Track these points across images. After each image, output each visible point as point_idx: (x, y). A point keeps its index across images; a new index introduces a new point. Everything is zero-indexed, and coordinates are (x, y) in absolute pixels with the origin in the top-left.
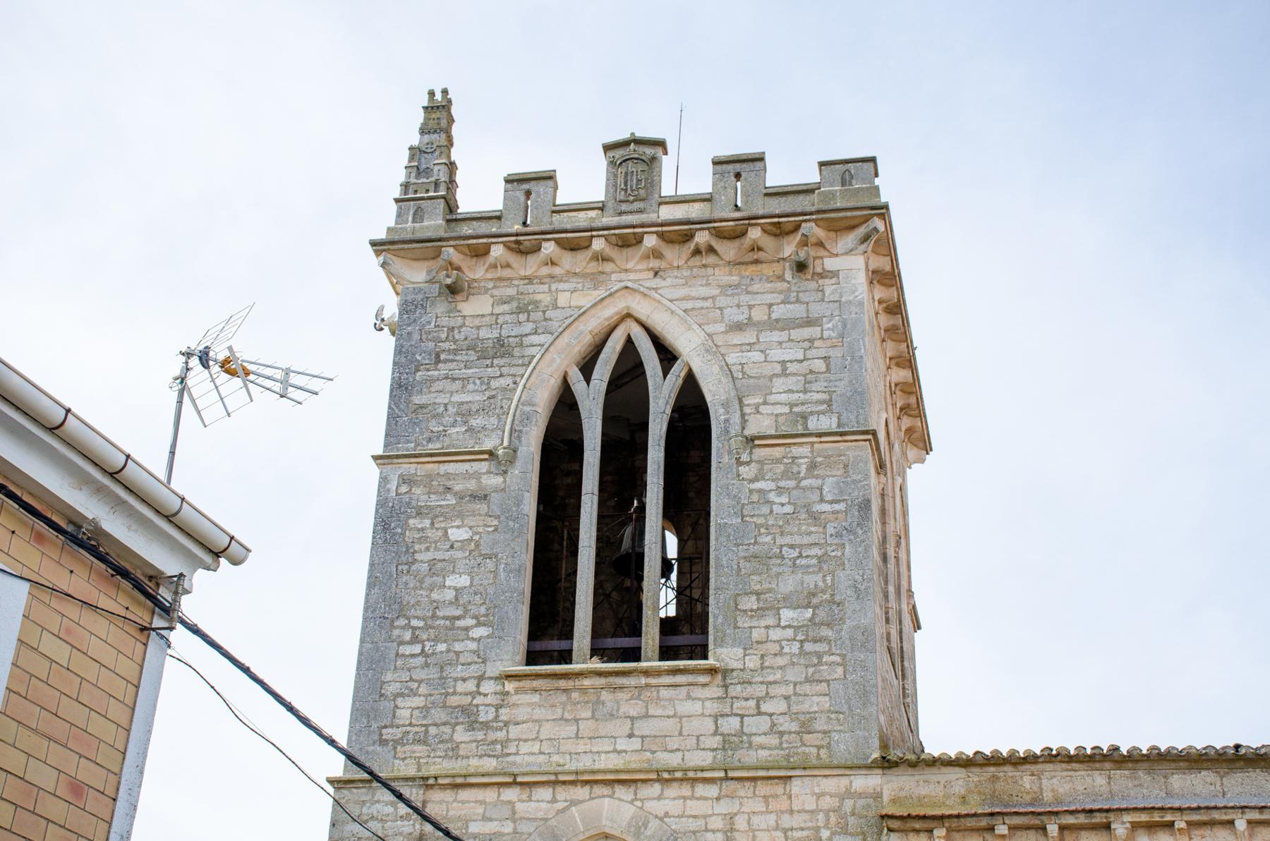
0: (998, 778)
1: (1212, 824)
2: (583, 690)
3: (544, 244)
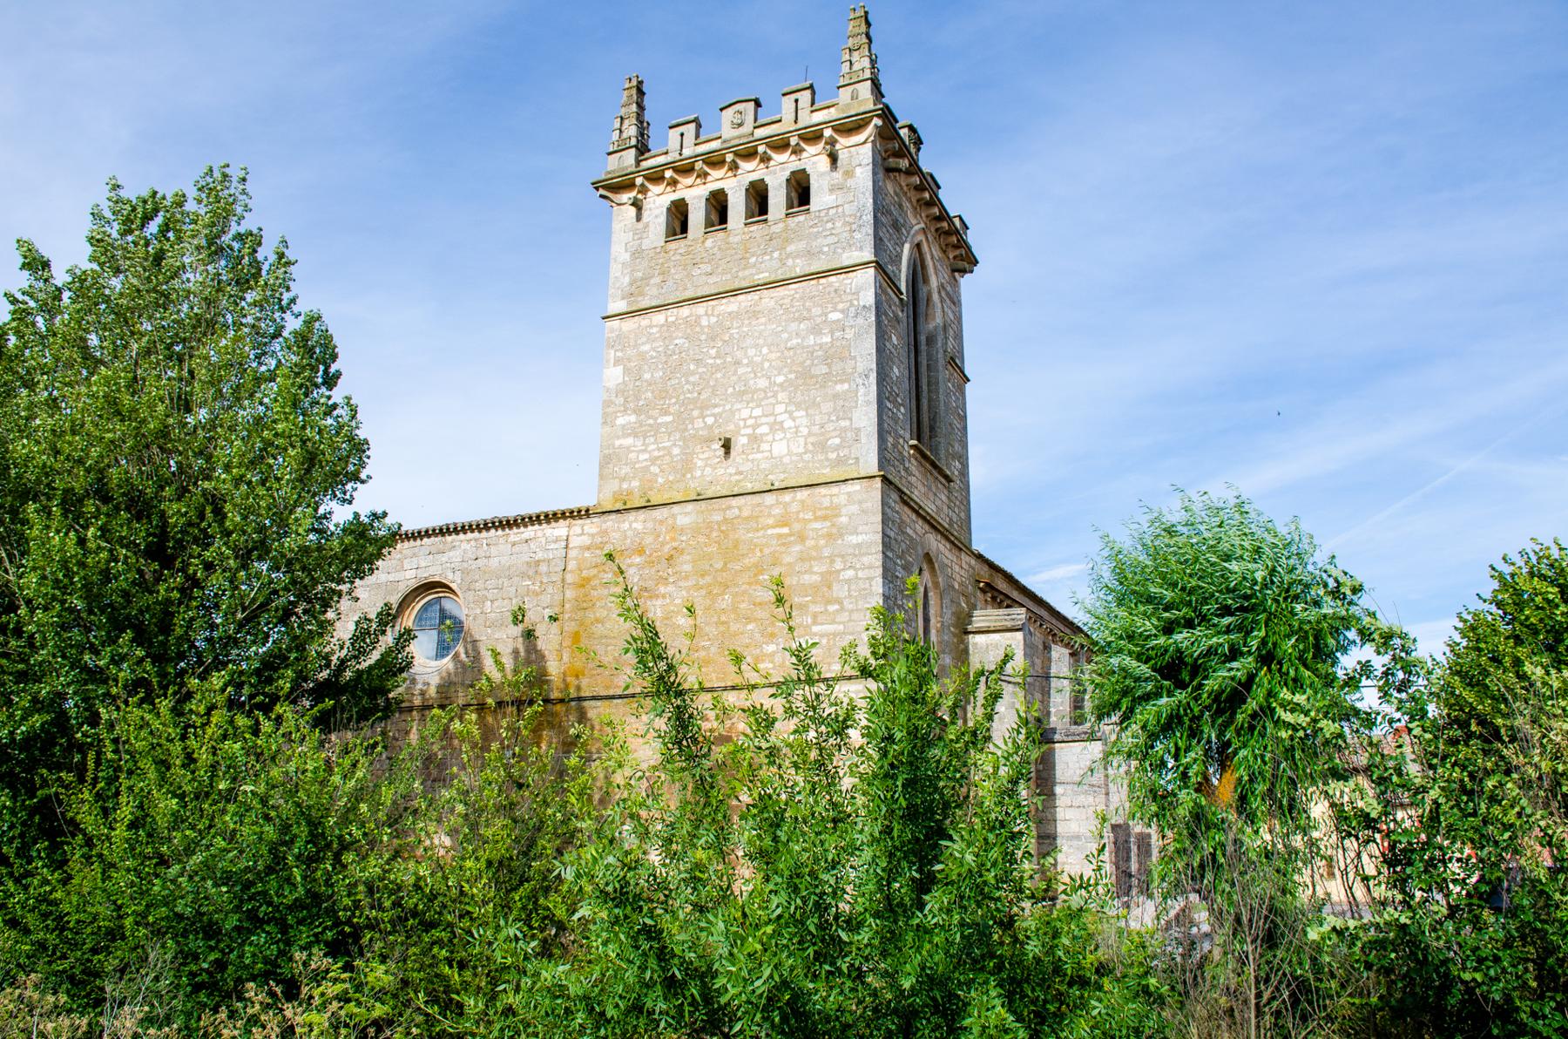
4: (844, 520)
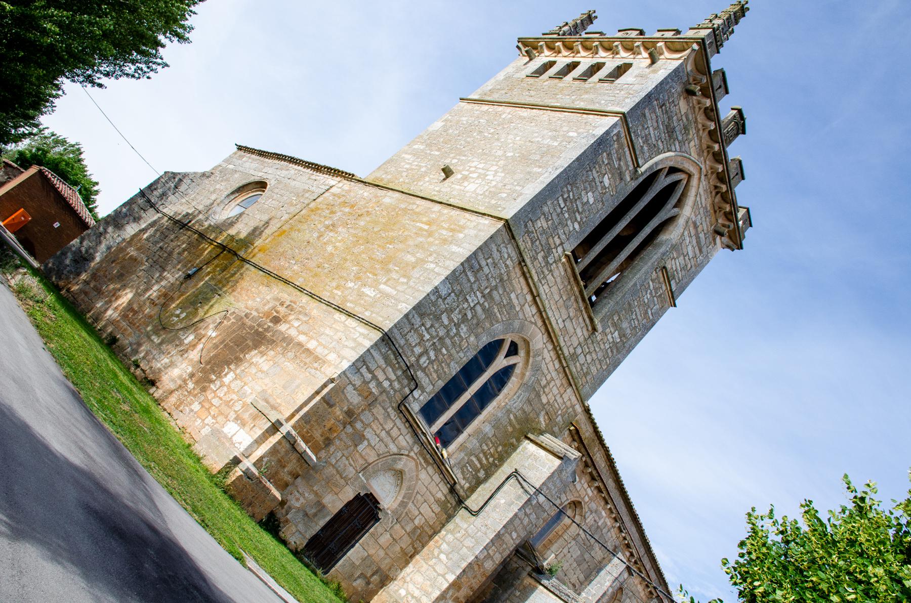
2: (572, 289)
3: (713, 124)
4: (461, 236)
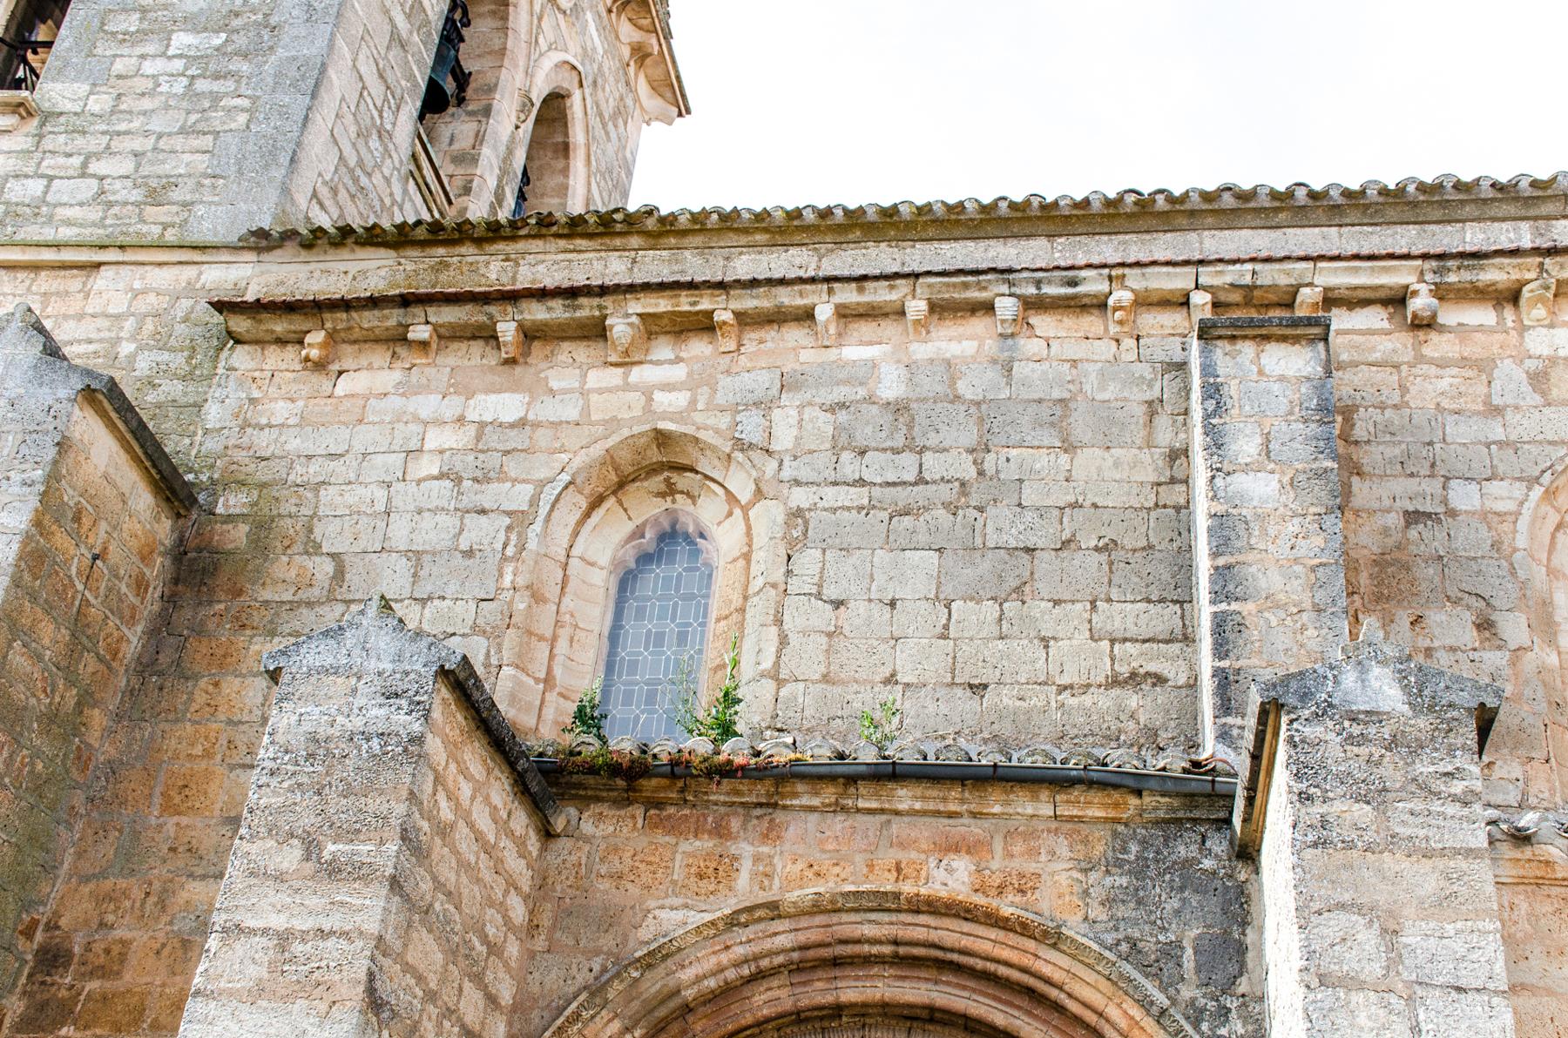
0: (447, 265)
1: (777, 318)
